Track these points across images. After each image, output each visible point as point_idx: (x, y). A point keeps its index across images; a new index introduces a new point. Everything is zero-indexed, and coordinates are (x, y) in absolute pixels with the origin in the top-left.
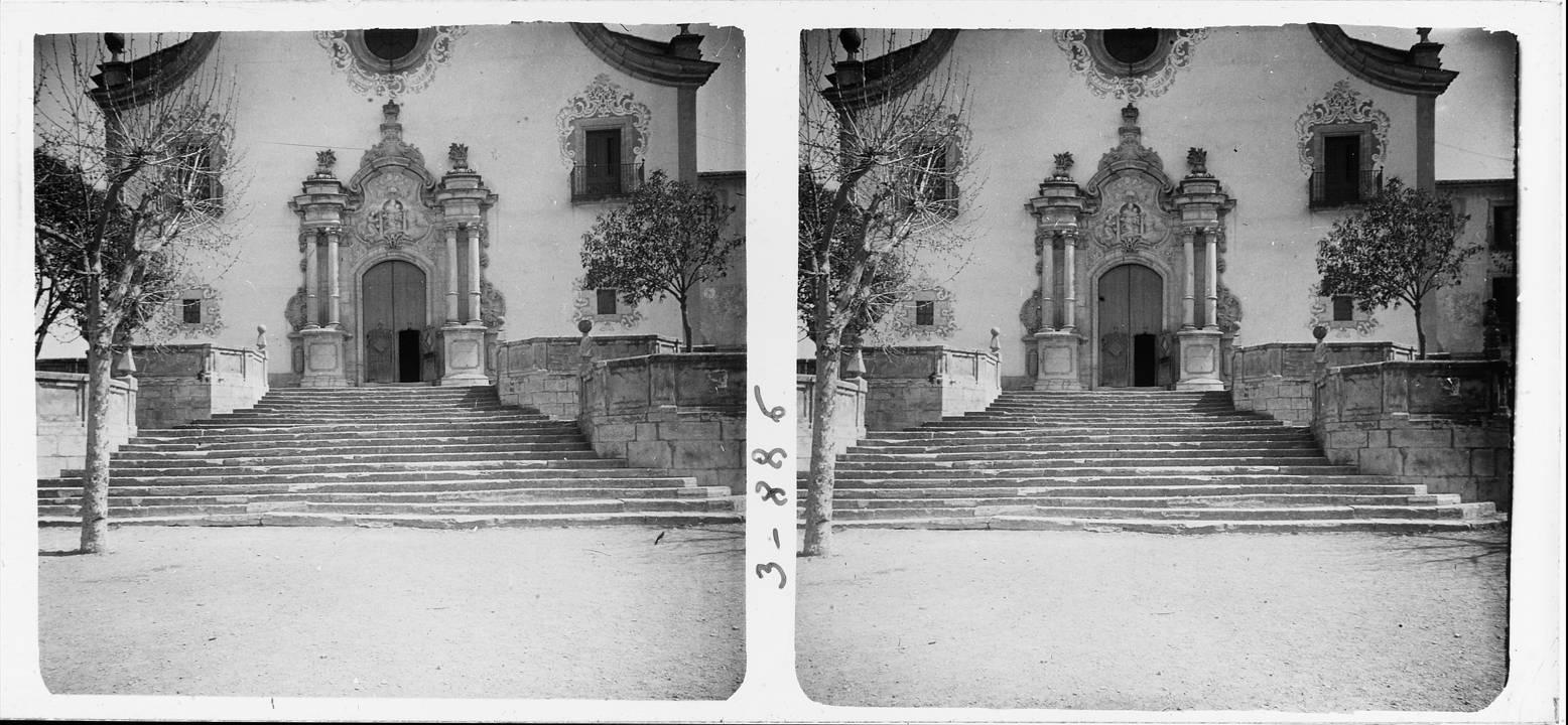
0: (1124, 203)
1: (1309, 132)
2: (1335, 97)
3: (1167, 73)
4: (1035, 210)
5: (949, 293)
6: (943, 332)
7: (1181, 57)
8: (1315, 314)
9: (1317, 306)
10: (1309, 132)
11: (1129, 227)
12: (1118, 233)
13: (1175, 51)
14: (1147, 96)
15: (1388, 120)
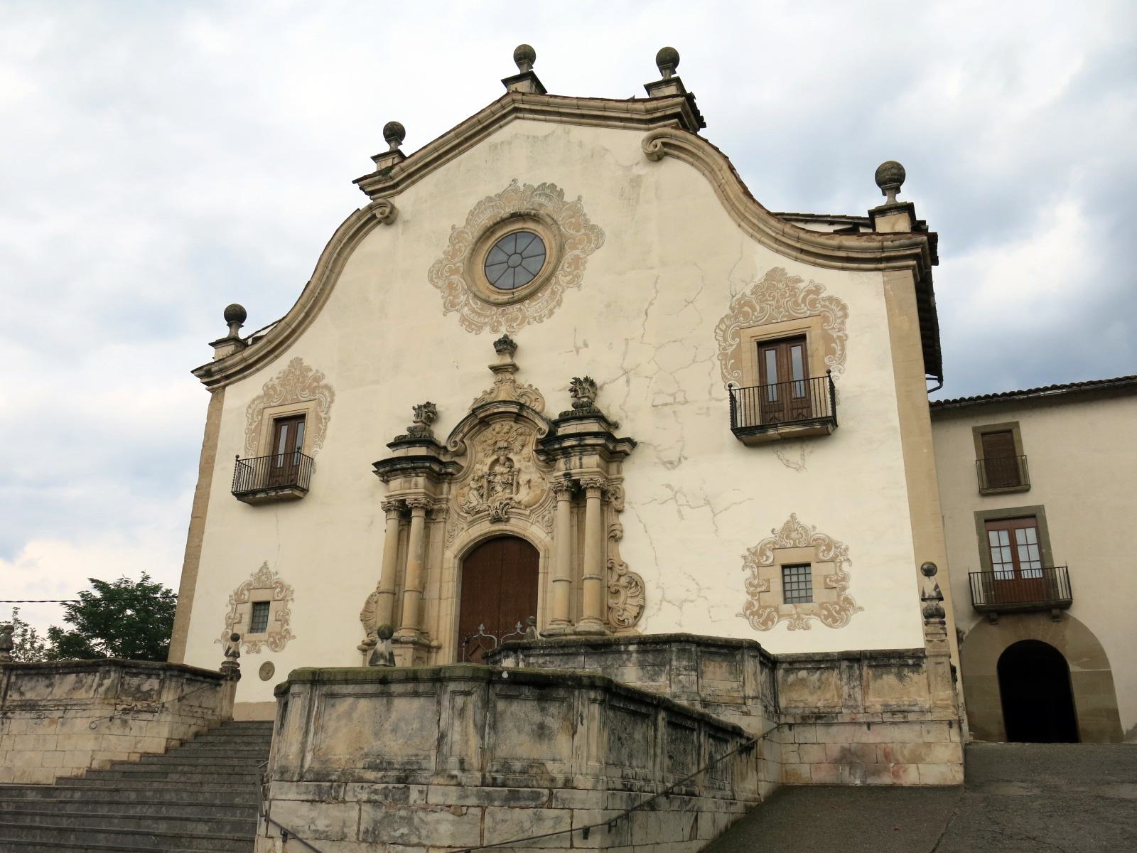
0: (495, 457)
1: (733, 339)
3: (553, 293)
5: (287, 589)
6: (274, 642)
7: (570, 273)
8: (753, 595)
9: (756, 582)
10: (733, 339)
11: (499, 488)
12: (485, 495)
13: (563, 268)
14: (529, 323)
15: (844, 308)
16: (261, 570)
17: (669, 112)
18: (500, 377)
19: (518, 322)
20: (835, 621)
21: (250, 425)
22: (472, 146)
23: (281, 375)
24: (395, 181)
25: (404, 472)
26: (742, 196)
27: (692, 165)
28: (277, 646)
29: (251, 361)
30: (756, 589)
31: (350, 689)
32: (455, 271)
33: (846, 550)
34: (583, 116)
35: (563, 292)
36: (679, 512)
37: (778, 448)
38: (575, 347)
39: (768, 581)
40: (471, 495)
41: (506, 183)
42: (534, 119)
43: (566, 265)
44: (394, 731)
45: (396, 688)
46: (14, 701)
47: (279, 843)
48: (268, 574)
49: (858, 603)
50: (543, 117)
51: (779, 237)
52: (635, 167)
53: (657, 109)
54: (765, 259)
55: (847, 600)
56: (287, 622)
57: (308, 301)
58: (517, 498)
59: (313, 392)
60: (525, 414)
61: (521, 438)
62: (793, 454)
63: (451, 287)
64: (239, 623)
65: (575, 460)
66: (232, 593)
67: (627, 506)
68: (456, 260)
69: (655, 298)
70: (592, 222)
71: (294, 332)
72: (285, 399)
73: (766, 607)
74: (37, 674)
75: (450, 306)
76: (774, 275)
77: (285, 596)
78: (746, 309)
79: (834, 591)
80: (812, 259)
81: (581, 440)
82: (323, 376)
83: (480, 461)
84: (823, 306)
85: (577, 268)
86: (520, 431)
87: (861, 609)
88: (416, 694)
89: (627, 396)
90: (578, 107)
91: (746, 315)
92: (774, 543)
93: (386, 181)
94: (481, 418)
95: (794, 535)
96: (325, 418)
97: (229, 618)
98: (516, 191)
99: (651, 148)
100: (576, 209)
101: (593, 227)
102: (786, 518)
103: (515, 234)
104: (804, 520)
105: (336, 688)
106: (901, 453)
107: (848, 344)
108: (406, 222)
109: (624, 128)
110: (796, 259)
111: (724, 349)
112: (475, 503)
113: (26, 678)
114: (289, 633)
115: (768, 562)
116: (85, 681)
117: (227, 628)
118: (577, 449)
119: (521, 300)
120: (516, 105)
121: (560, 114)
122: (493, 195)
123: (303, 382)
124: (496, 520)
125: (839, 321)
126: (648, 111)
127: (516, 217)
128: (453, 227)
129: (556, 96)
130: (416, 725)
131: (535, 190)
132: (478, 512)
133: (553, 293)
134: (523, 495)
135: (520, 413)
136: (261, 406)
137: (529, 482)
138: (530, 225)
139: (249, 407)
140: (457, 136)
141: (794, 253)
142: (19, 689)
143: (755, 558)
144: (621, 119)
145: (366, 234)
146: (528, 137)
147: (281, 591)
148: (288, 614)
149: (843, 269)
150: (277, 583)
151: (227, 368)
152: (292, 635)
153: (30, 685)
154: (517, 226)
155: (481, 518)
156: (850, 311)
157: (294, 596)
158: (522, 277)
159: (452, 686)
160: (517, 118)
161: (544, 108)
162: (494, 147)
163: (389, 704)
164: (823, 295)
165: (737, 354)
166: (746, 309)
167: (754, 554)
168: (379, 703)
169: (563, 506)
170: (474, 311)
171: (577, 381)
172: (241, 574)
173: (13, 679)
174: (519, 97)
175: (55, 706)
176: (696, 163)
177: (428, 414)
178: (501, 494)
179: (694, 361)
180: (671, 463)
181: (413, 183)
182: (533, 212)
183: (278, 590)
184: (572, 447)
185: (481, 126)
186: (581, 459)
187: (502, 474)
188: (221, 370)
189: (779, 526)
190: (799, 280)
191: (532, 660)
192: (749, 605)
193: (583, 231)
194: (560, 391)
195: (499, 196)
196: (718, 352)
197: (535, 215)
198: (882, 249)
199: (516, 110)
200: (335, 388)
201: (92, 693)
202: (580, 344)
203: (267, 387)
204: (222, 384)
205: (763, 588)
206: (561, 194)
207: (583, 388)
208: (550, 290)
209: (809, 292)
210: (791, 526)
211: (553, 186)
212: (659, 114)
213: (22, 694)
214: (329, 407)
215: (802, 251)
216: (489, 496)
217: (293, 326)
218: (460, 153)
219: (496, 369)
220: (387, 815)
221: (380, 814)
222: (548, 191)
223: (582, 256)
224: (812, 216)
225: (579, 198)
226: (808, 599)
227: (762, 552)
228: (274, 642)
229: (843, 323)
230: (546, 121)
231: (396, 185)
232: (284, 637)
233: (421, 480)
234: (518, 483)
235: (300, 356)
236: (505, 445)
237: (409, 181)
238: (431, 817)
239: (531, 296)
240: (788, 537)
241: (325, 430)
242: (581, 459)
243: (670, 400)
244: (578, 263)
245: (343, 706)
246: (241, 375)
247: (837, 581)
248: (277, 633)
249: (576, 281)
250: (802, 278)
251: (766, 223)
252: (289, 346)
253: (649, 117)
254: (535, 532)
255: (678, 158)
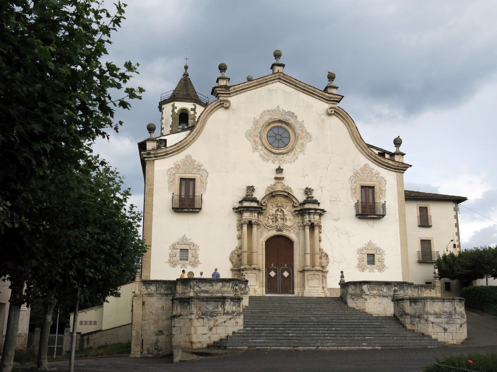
1: (354, 184)
2: (364, 170)
4: (239, 211)
5: (196, 246)
6: (193, 264)
7: (300, 148)
8: (360, 262)
9: (360, 258)
10: (354, 184)
11: (279, 220)
12: (274, 222)
13: (298, 145)
14: (286, 163)
15: (385, 181)
16: (183, 237)
17: (335, 100)
18: (278, 181)
19: (282, 161)
20: (381, 270)
21: (170, 179)
22: (261, 87)
23: (182, 161)
24: (230, 92)
25: (251, 211)
26: (360, 138)
27: (342, 121)
28: (194, 266)
29: (169, 153)
30: (360, 260)
31: (437, 300)
32: (257, 136)
33: (384, 251)
34: (304, 90)
35: (298, 154)
36: (339, 235)
37: (367, 220)
38: (303, 175)
39: (363, 258)
40: (269, 221)
41: (275, 107)
42: (286, 84)
43: (299, 145)
44: (446, 307)
45: (445, 301)
46: (198, 290)
47: (431, 324)
48: (187, 240)
49: (387, 266)
50: (289, 85)
51: (369, 154)
52: (322, 115)
53: (332, 98)
54: (363, 160)
55: (384, 265)
56: (197, 257)
57: (195, 133)
58: (286, 224)
59: (199, 170)
60: (289, 196)
61: (286, 204)
62: (371, 222)
63: (255, 141)
64: (175, 256)
65: (312, 216)
66: (171, 245)
67: (322, 231)
68: (256, 132)
69: (330, 164)
70: (308, 131)
71: (187, 144)
72: (185, 171)
73: (363, 265)
74: (206, 282)
75: (256, 149)
76: (366, 165)
77: (196, 248)
78: (358, 175)
79: (381, 263)
80: (378, 164)
81: (316, 211)
82: (202, 166)
83: (271, 210)
84: (380, 179)
85: (303, 147)
86: (286, 201)
87: (387, 268)
88: (449, 302)
89: (322, 195)
90: (304, 87)
91: (358, 177)
92: (365, 248)
93: (226, 91)
94: (272, 195)
95: (371, 246)
96: (205, 183)
97: (171, 254)
98: (279, 111)
99: (329, 111)
100: (302, 125)
101: (308, 133)
102: (369, 241)
103: (278, 127)
104: (374, 242)
105: (435, 300)
106: (399, 227)
107: (386, 192)
108: (233, 110)
109: (319, 99)
110: (373, 162)
111: (352, 186)
112: (271, 224)
113: (200, 283)
114: (199, 262)
115: (364, 253)
116: (226, 285)
117: (170, 258)
118: (313, 213)
119: (283, 154)
120: (280, 77)
121: (296, 86)
122: (270, 110)
123: (193, 166)
124: (280, 230)
125: (384, 185)
126: (329, 97)
127: (280, 121)
128: (254, 118)
129: (297, 80)
130: (449, 306)
131: (286, 113)
132: (273, 227)
133: (295, 154)
134: (288, 223)
135: (288, 196)
136: (174, 172)
137: (290, 219)
138: (287, 128)
139: (168, 171)
140: (257, 82)
141: (373, 161)
142: (198, 286)
143: (360, 251)
144: (318, 96)
145: (216, 110)
146: (283, 91)
147: (194, 246)
148: (198, 255)
149: (386, 169)
150: (191, 243)
151: (158, 153)
152: (200, 262)
153: (202, 285)
154: (279, 124)
155: (273, 229)
156: (387, 182)
157: (199, 248)
158: (281, 144)
159: (456, 301)
160: (279, 81)
161: (291, 82)
162: (270, 90)
163: (444, 303)
164: (380, 176)
165: (355, 189)
166: (358, 175)
167: (360, 250)
168: (442, 303)
169: (307, 230)
170: (265, 153)
171: (307, 188)
172: (175, 239)
173: (195, 283)
174: (282, 75)
175: (216, 292)
176: (344, 121)
177: (251, 189)
178: (280, 222)
179: (342, 188)
180: (336, 220)
181: (237, 94)
182: (287, 122)
183: (192, 246)
184: (312, 212)
185: (266, 81)
186: (314, 216)
187: (280, 215)
188: (155, 154)
189: (367, 243)
190: (373, 169)
191: (371, 286)
192: (359, 265)
193: (305, 134)
194: (299, 189)
195: (273, 111)
196: (350, 187)
197: (287, 123)
198: (398, 166)
199: (279, 78)
200: (208, 171)
201: (230, 289)
202: (305, 175)
203: (176, 164)
204: (154, 159)
205: (362, 260)
206: (296, 117)
207: (308, 191)
208: (293, 153)
209: (376, 174)
210: (370, 244)
211: (293, 113)
212: (332, 99)
213: (200, 288)
214: (206, 178)
215: (375, 160)
216: (276, 222)
217: (188, 142)
218: (256, 88)
219: (276, 178)
220: (450, 320)
221: (448, 320)
222: (291, 115)
223: (304, 143)
224: (373, 146)
225: (303, 121)
226: (374, 264)
227: (362, 250)
228: (193, 264)
229: (385, 185)
230: (290, 86)
231: (230, 94)
232: (197, 263)
233: (256, 215)
234: (286, 219)
235: (190, 155)
236: (281, 205)
237: (236, 93)
238: (457, 320)
239: (286, 153)
240: (369, 246)
241: (206, 187)
242: (314, 216)
243: (335, 200)
244: (303, 145)
245: (436, 303)
246: (163, 157)
247: (382, 260)
248: (194, 262)
249: (302, 151)
250: (374, 169)
251: (366, 149)
252: (185, 149)
253: (329, 99)
254: (292, 236)
255: (337, 116)
